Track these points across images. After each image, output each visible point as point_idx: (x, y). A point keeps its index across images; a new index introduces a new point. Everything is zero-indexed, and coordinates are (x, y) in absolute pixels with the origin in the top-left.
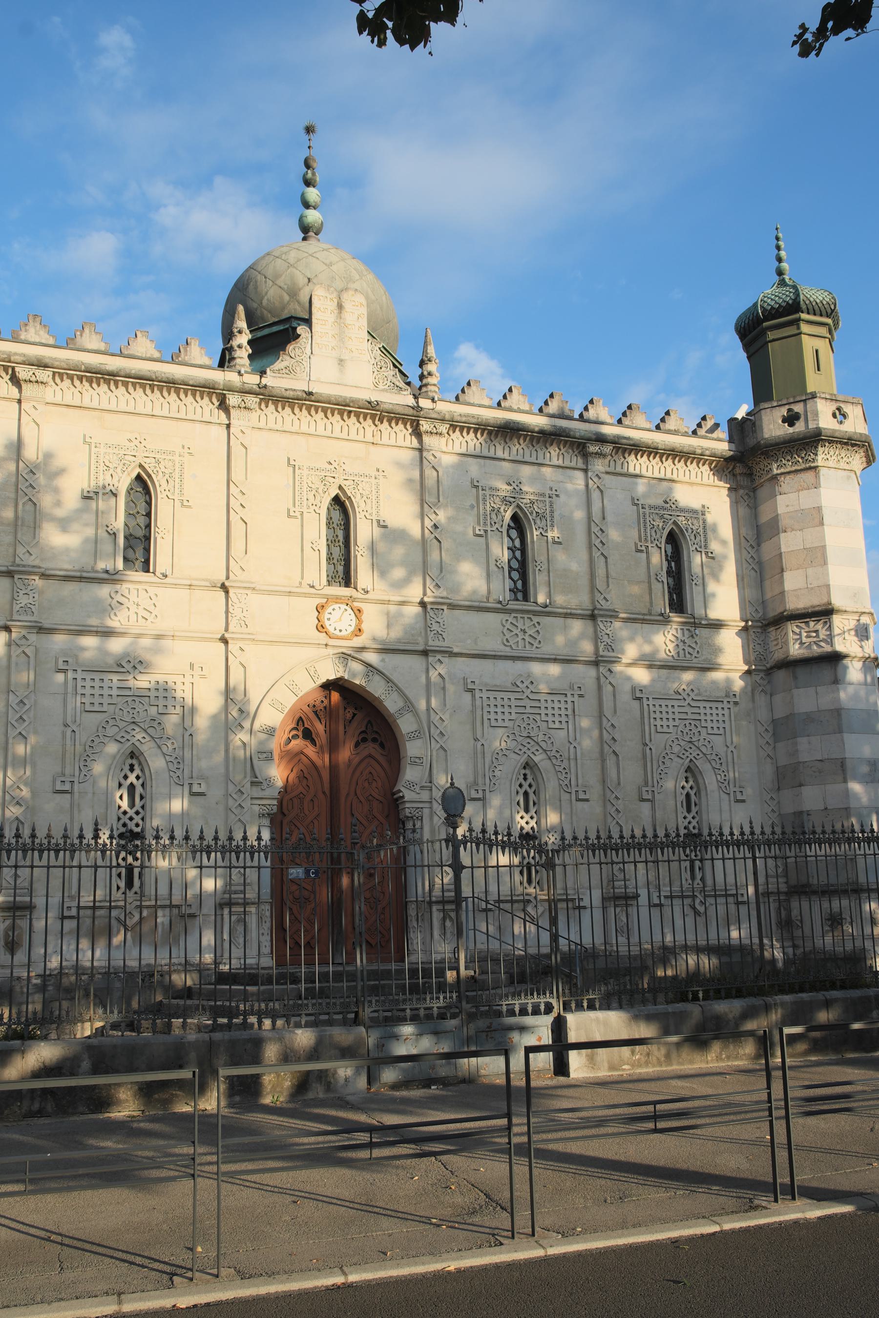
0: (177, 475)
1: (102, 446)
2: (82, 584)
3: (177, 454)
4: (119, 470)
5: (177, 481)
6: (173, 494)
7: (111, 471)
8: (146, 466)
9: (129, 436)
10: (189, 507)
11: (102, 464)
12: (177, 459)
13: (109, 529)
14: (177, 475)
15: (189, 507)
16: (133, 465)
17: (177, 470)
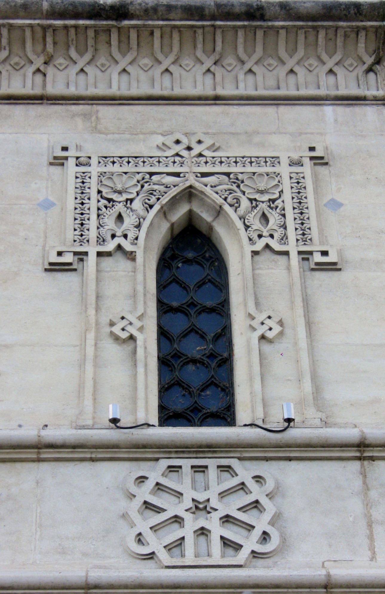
0: (288, 201)
1: (94, 161)
2: (44, 466)
3: (285, 161)
4: (137, 205)
5: (290, 214)
6: (284, 239)
7: (119, 208)
8: (208, 190)
9: (159, 140)
10: (333, 267)
11: (94, 196)
12: (284, 170)
13: (117, 330)
14: (288, 201)
15: (333, 267)
16: (173, 192)
17: (287, 196)
